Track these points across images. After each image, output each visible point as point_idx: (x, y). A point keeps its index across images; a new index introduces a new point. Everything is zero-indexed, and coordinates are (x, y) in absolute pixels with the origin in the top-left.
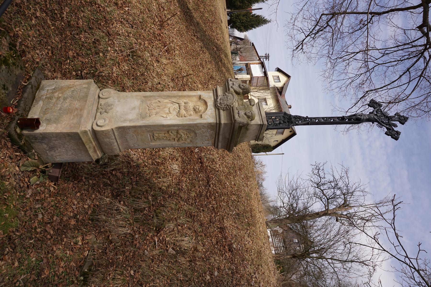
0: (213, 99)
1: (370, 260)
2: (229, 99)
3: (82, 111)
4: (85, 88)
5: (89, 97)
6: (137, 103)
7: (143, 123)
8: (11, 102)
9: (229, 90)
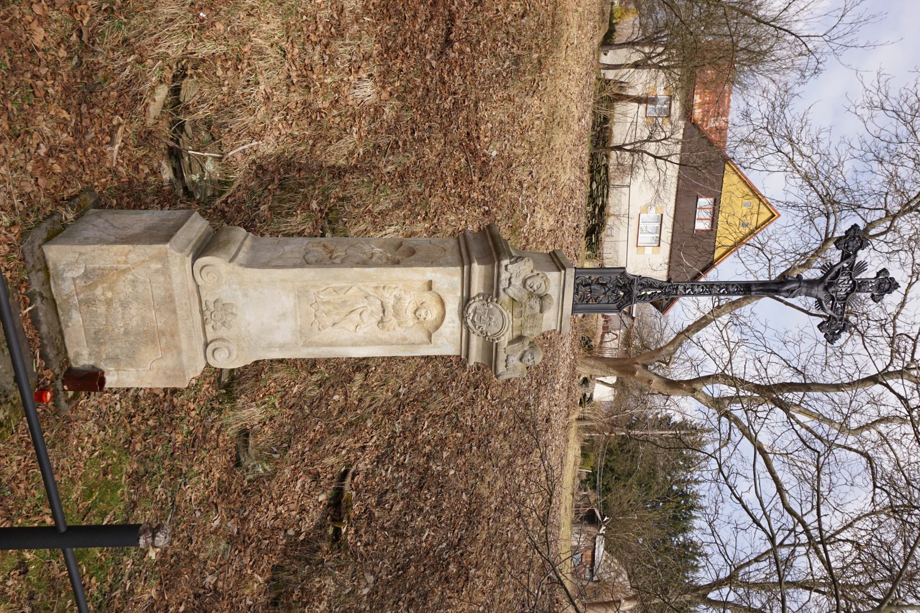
0: (459, 294)
1: (721, 331)
2: (495, 322)
3: (176, 338)
4: (157, 271)
5: (176, 299)
6: (288, 302)
7: (308, 354)
8: (35, 370)
9: (498, 295)
